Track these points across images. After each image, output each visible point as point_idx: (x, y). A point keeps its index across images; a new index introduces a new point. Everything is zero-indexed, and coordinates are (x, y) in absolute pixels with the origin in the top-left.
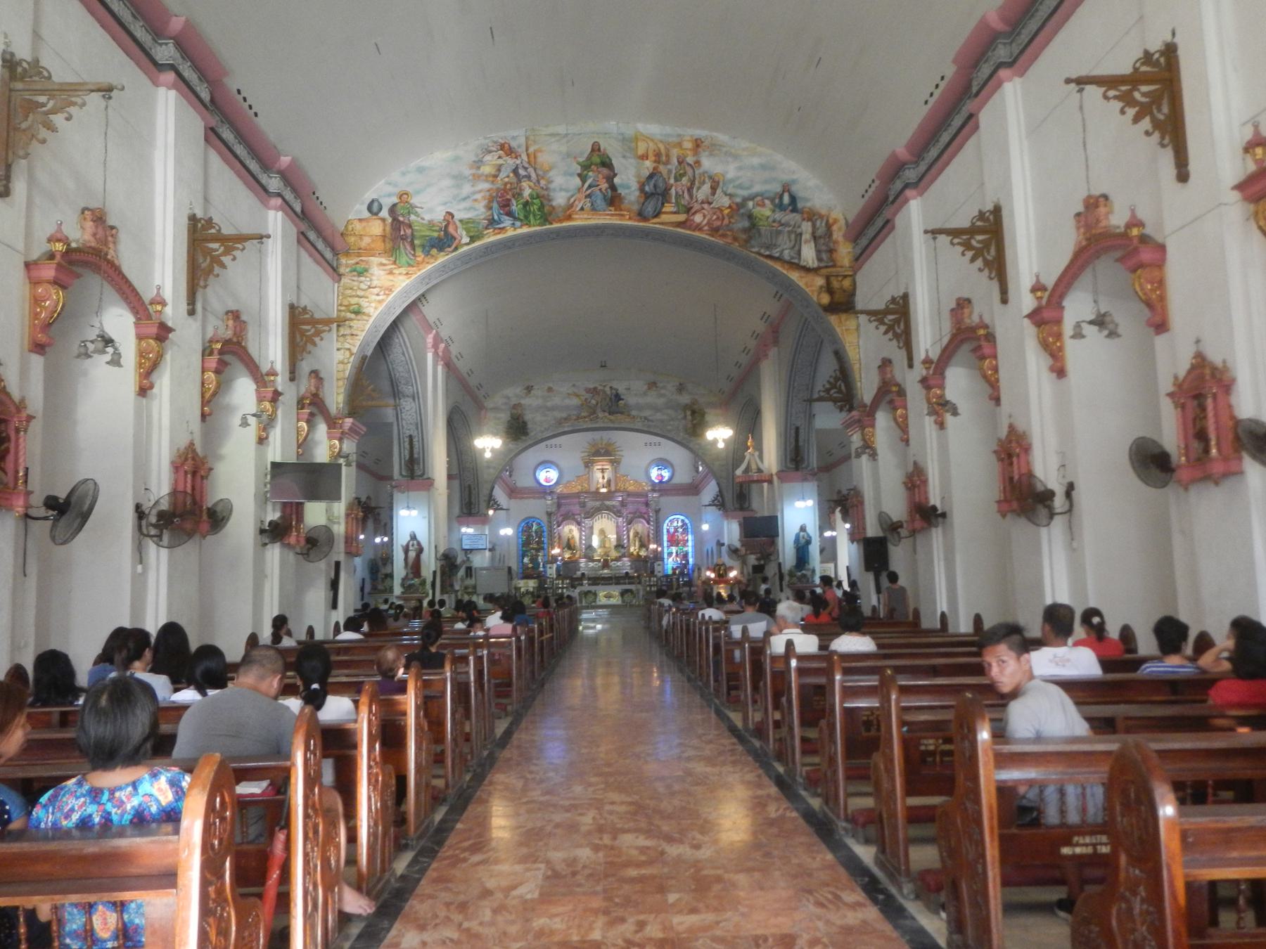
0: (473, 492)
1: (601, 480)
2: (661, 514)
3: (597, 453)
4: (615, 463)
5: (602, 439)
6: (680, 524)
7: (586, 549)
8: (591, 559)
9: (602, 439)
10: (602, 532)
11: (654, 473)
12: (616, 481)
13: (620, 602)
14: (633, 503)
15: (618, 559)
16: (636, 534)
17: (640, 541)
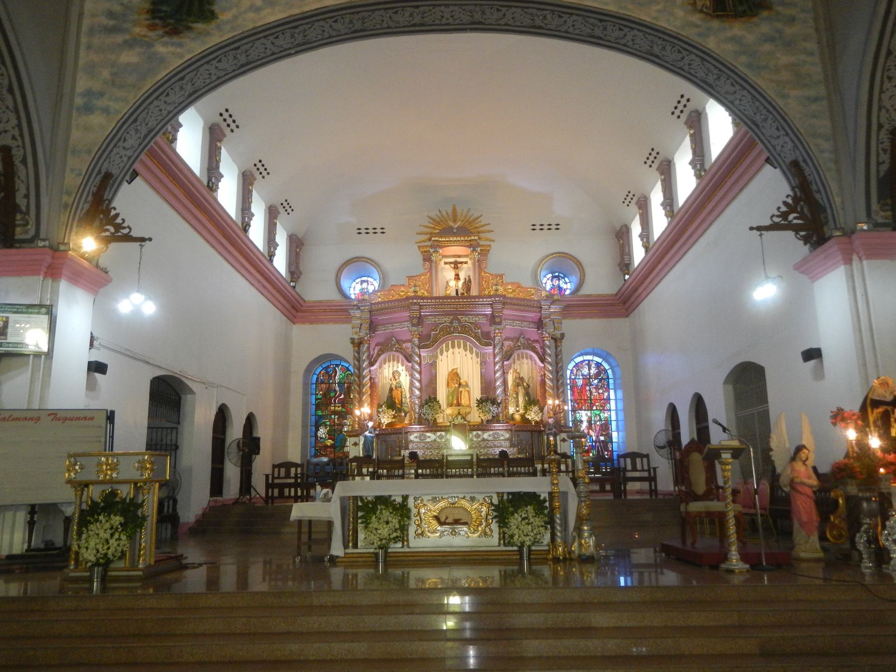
0: (21, 171)
1: (452, 283)
2: (565, 344)
3: (447, 231)
4: (482, 253)
5: (454, 210)
6: (593, 371)
7: (421, 406)
8: (434, 427)
9: (454, 210)
10: (454, 376)
11: (548, 283)
12: (480, 284)
13: (493, 541)
14: (514, 319)
15: (482, 427)
16: (519, 381)
17: (527, 394)
